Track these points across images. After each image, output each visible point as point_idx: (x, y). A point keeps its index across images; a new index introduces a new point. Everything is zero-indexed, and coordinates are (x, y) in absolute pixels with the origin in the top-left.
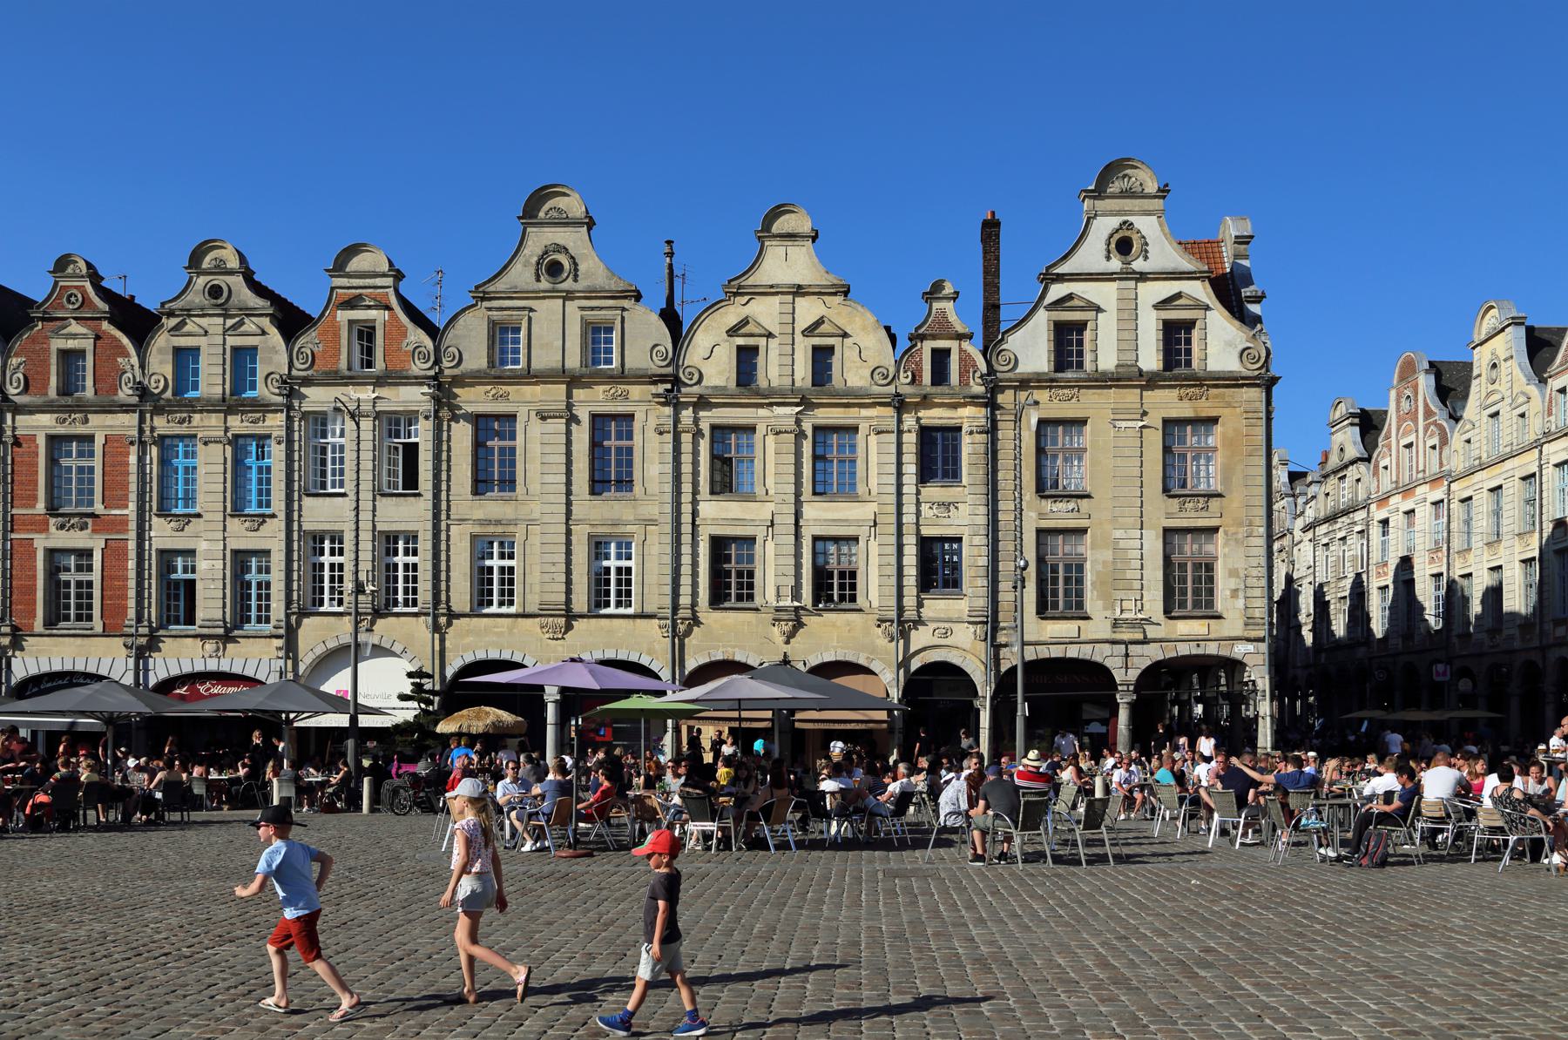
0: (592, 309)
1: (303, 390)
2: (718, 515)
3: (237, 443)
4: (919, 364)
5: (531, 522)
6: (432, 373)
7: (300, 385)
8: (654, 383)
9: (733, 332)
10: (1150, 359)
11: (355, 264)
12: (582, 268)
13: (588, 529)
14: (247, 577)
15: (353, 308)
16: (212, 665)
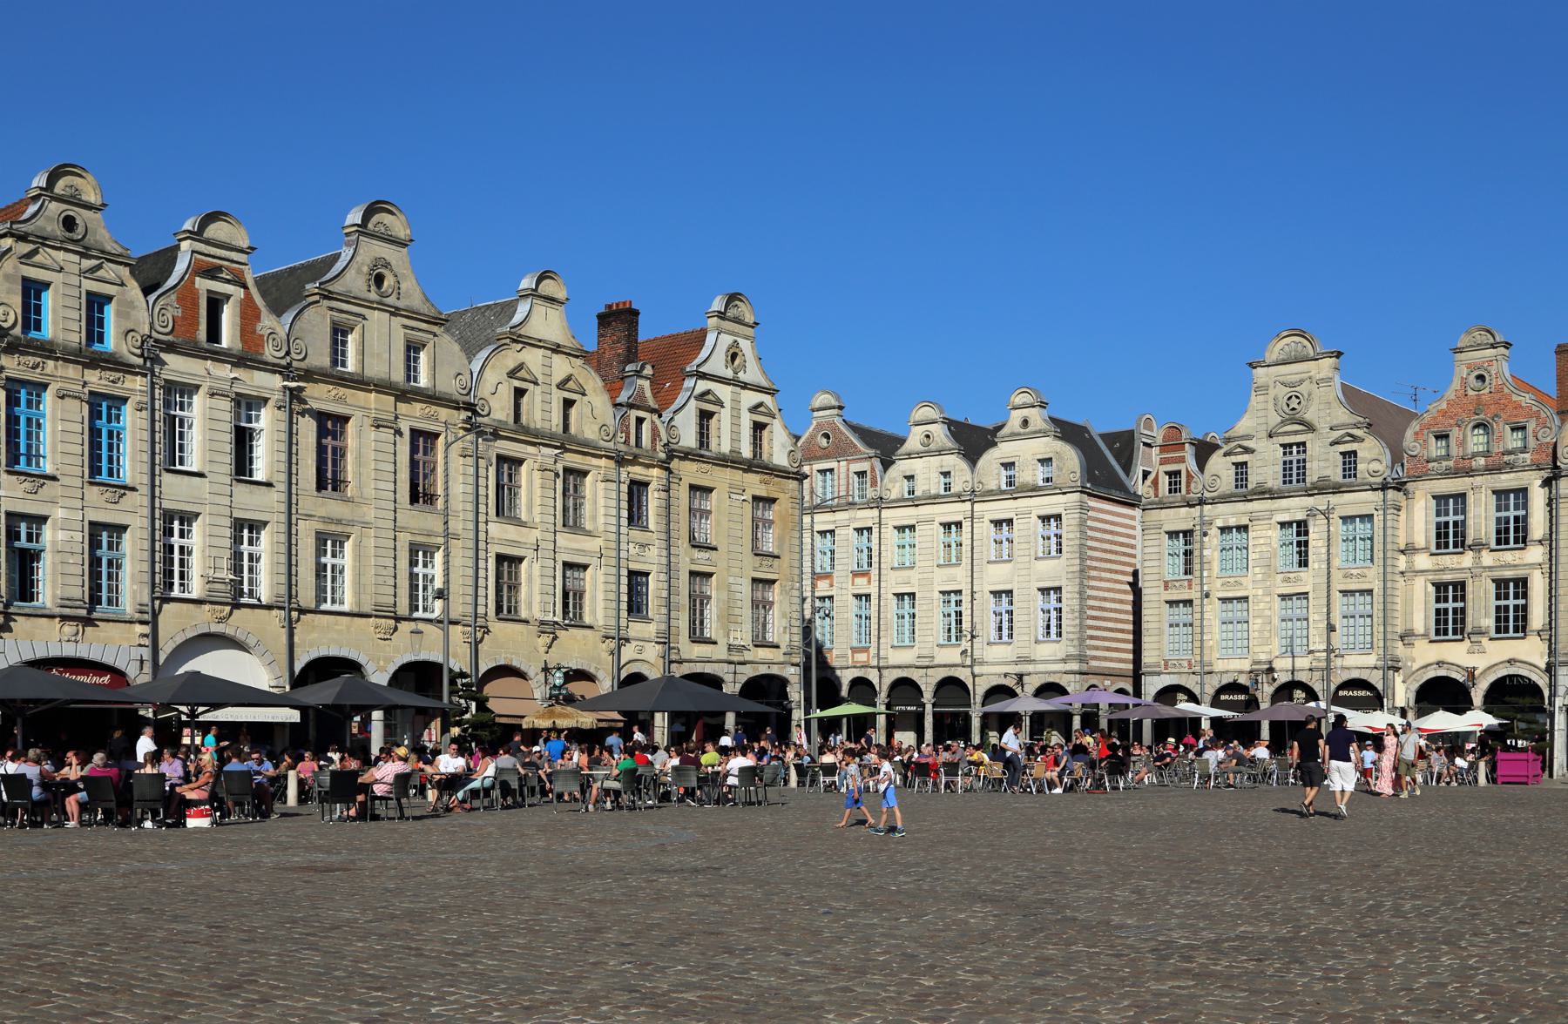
0: (413, 329)
1: (163, 356)
2: (500, 535)
3: (95, 401)
4: (628, 427)
5: (366, 525)
6: (283, 362)
7: (162, 350)
8: (458, 409)
9: (512, 374)
10: (747, 452)
11: (216, 230)
12: (403, 286)
13: (409, 537)
14: (323, 560)
15: (214, 278)
16: (69, 651)
